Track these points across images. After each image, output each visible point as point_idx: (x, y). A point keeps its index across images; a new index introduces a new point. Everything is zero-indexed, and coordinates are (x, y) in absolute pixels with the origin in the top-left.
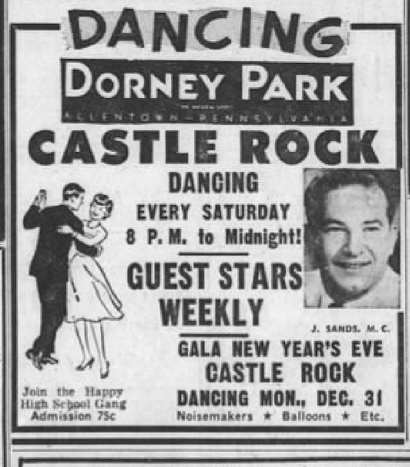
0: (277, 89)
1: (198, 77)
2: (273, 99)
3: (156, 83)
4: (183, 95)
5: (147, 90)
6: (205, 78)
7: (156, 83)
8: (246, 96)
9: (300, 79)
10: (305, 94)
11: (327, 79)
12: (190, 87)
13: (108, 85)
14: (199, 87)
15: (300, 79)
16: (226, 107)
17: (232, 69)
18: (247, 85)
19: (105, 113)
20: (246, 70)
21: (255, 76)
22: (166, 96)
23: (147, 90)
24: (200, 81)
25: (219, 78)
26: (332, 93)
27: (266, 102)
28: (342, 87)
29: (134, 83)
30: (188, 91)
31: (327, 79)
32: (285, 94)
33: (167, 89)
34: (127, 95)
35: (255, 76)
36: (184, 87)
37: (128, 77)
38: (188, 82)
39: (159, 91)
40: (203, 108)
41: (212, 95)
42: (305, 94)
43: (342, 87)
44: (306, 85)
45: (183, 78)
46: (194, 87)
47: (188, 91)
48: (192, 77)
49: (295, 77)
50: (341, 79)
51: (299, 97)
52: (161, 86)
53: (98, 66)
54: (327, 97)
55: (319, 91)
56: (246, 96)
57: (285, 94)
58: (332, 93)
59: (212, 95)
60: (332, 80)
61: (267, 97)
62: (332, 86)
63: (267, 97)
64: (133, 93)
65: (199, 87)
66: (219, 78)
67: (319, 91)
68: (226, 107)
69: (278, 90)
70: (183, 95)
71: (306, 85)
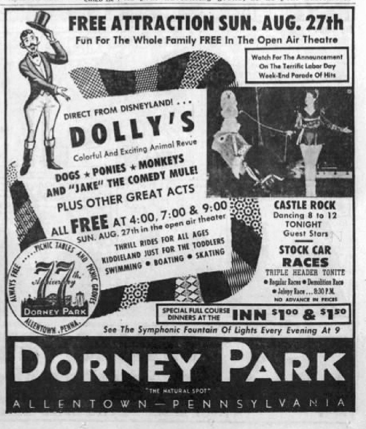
0: (263, 369)
1: (170, 357)
2: (257, 380)
3: (120, 364)
4: (152, 377)
5: (110, 371)
6: (178, 358)
7: (120, 364)
8: (226, 377)
9: (290, 357)
10: (295, 375)
11: (321, 356)
12: (160, 368)
13: (64, 367)
15: (290, 357)
16: (203, 391)
17: (210, 348)
18: (228, 365)
19: (60, 401)
20: (227, 348)
21: (236, 355)
22: (132, 378)
23: (110, 371)
24: (173, 361)
25: (195, 358)
26: (327, 372)
28: (337, 365)
29: (95, 364)
30: (157, 373)
31: (321, 356)
32: (272, 374)
33: (134, 371)
34: (87, 378)
35: (236, 355)
36: (152, 368)
37: (88, 358)
38: (158, 363)
39: (124, 373)
41: (187, 377)
42: (295, 375)
43: (337, 365)
45: (152, 358)
46: (164, 368)
47: (157, 373)
48: (164, 357)
50: (337, 357)
51: (289, 377)
52: (127, 367)
53: (52, 345)
54: (321, 377)
55: (312, 370)
56: (226, 377)
57: (272, 374)
58: (327, 373)
59: (187, 377)
60: (326, 359)
61: (251, 378)
62: (327, 365)
63: (251, 378)
66: (195, 358)
67: (312, 370)
68: (203, 391)
69: (264, 370)
70: (152, 377)
71: (297, 364)
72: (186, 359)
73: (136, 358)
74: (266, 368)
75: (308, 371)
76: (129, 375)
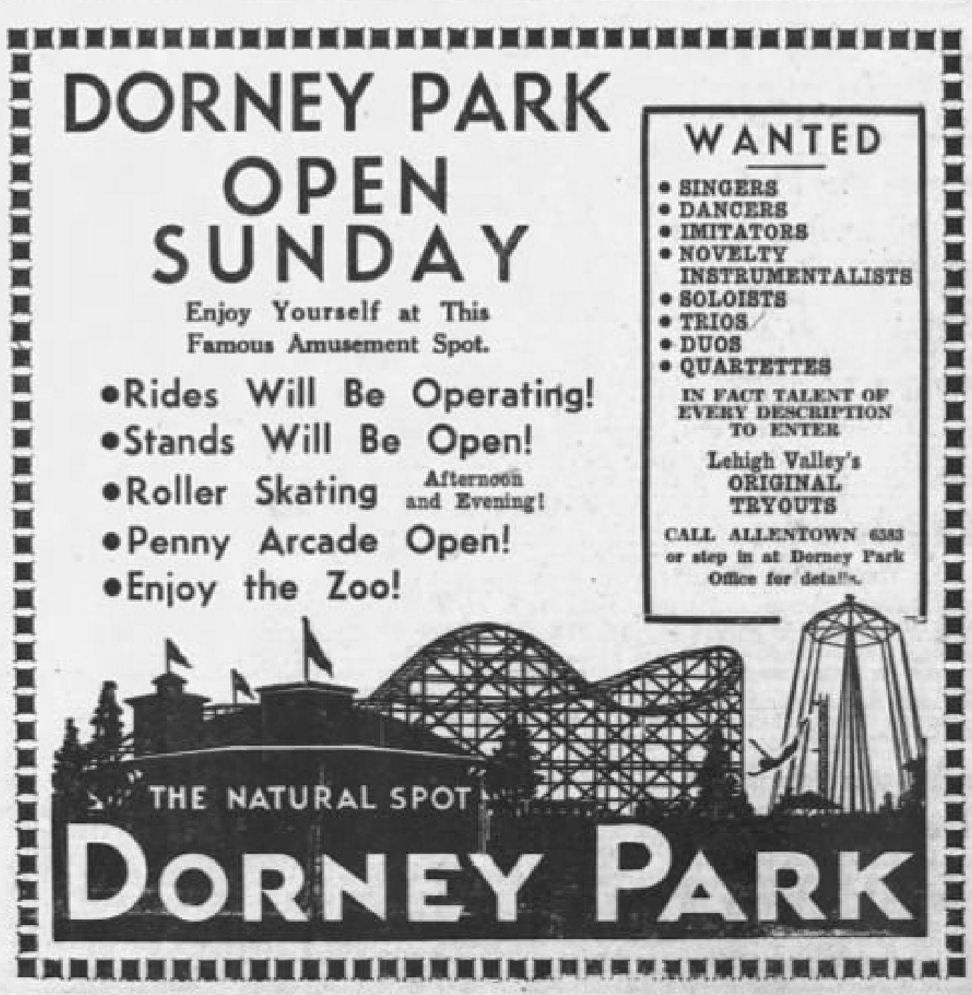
0: (701, 893)
1: (465, 861)
6: (483, 862)
9: (769, 863)
12: (439, 888)
14: (467, 887)
15: (769, 863)
18: (611, 881)
20: (609, 839)
25: (528, 863)
26: (865, 899)
27: (665, 923)
29: (272, 879)
30: (431, 900)
31: (849, 860)
32: (722, 902)
36: (419, 888)
37: (254, 865)
38: (431, 874)
40: (488, 837)
41: (507, 910)
44: (787, 878)
45: (418, 863)
46: (449, 888)
47: (431, 900)
48: (450, 862)
49: (754, 859)
50: (890, 861)
56: (607, 910)
58: (865, 899)
59: (507, 910)
60: (863, 865)
62: (863, 879)
64: (267, 904)
65: (467, 887)
66: (528, 863)
71: (787, 878)
72: (506, 866)
73: (376, 863)
74: (708, 888)
75: (814, 897)
76: (361, 906)
